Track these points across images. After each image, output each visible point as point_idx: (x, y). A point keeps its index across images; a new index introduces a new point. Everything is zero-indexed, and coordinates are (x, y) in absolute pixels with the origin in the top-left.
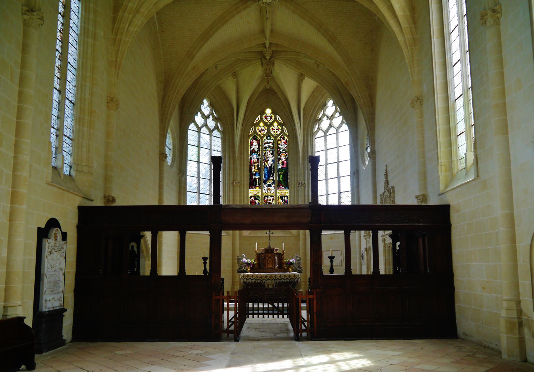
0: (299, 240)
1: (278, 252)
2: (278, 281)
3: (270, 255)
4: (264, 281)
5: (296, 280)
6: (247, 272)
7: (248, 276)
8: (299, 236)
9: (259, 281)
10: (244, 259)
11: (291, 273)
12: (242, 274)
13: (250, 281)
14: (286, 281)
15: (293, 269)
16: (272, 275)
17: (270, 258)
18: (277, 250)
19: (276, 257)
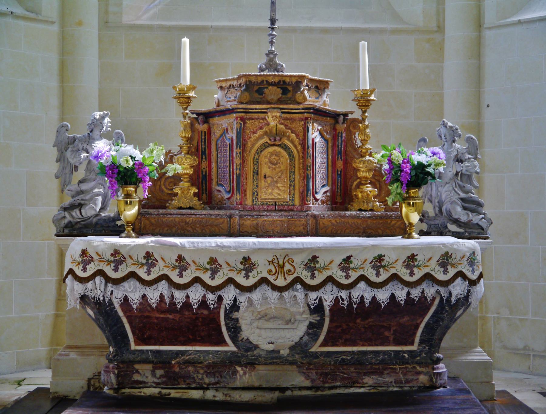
0: (439, 49)
1: (328, 101)
2: (328, 296)
3: (273, 119)
4: (229, 294)
5: (458, 289)
6: (118, 231)
7: (118, 257)
8: (440, 29)
9: (196, 294)
10: (101, 146)
11: (418, 240)
12: (78, 244)
13: (133, 292)
14: (383, 296)
15: (423, 218)
16: (288, 255)
17: (275, 138)
18: (320, 87)
19: (314, 134)
